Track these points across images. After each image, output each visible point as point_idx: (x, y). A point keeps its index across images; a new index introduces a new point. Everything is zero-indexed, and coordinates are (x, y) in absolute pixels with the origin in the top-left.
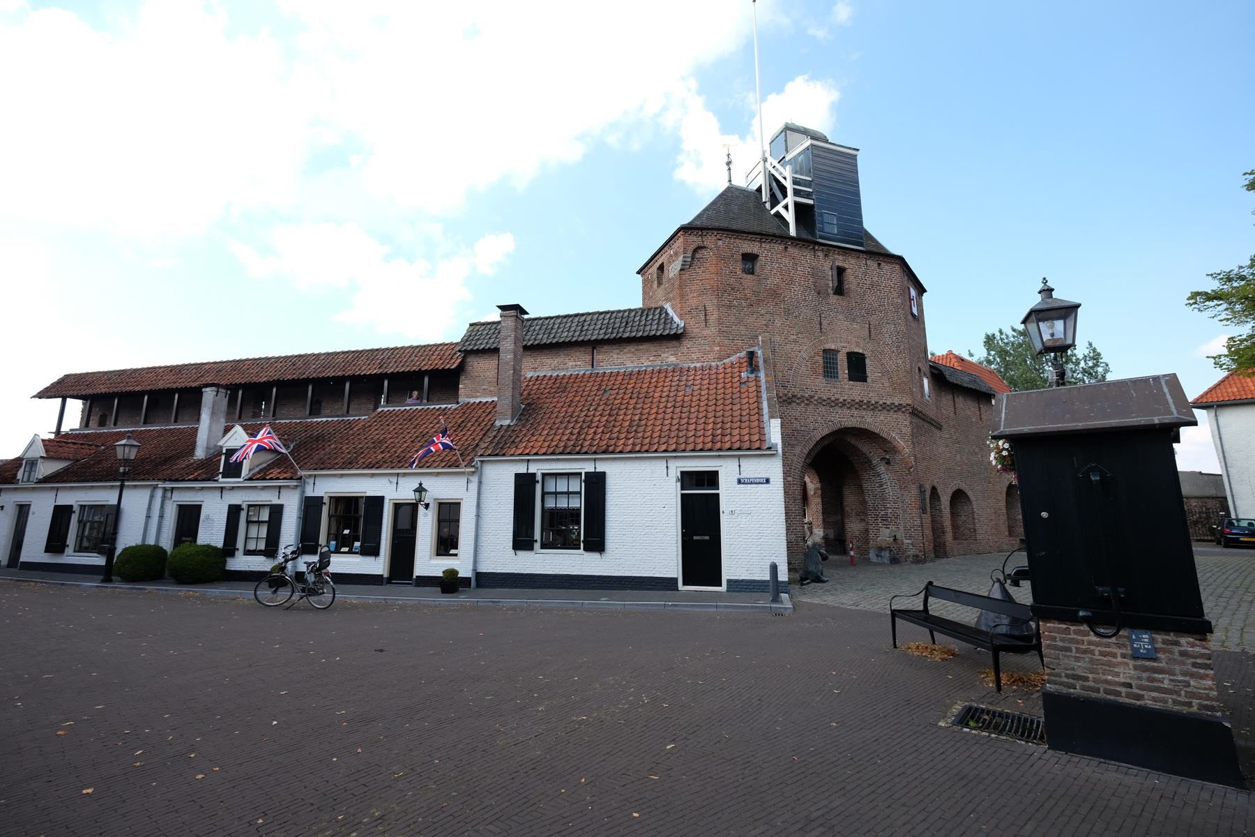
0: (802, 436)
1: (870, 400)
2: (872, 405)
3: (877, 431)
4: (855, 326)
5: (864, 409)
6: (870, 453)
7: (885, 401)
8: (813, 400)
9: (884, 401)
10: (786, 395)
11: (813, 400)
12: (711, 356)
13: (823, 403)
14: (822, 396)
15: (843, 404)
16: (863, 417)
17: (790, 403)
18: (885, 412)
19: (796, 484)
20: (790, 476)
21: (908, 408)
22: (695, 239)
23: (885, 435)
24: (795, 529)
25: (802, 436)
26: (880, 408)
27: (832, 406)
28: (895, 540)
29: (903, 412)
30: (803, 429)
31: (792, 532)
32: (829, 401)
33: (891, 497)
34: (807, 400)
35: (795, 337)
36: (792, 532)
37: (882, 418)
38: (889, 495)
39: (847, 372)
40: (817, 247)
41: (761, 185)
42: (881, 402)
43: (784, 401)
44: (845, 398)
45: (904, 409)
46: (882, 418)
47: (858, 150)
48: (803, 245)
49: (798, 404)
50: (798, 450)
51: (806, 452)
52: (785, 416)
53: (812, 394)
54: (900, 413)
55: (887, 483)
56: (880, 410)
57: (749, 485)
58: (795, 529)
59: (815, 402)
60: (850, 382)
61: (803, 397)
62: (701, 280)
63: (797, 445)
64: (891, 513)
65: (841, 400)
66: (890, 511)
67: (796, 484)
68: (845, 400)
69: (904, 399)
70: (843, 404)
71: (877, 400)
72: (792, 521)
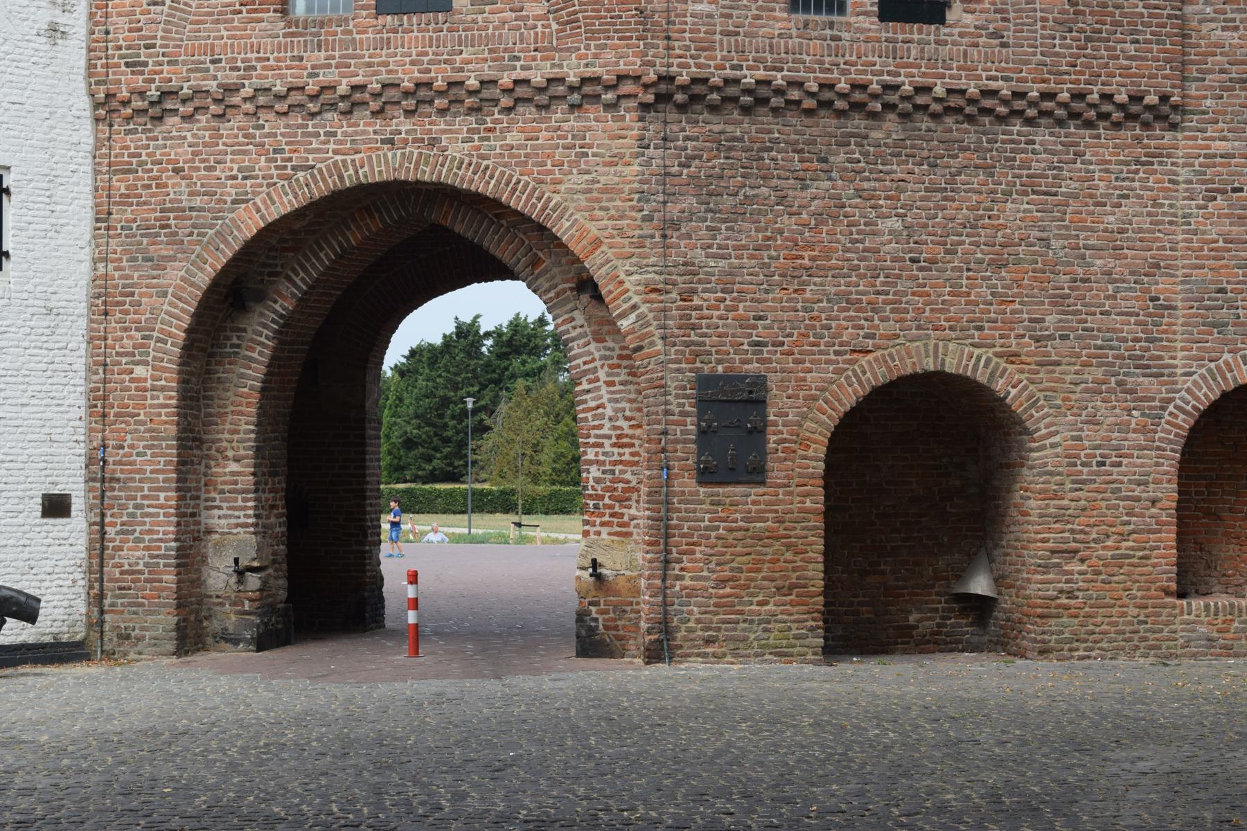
0: (194, 226)
1: (457, 76)
2: (472, 93)
3: (487, 188)
5: (442, 112)
7: (523, 75)
8: (236, 100)
9: (520, 74)
10: (142, 94)
11: (236, 100)
13: (277, 107)
14: (266, 83)
15: (353, 102)
16: (433, 142)
17: (159, 119)
18: (529, 112)
19: (163, 389)
20: (146, 363)
21: (627, 88)
23: (518, 203)
24: (150, 532)
25: (194, 226)
26: (506, 101)
27: (313, 115)
28: (598, 577)
29: (611, 106)
30: (198, 201)
31: (137, 540)
32: (296, 98)
33: (608, 425)
34: (217, 101)
36: (137, 540)
37: (513, 138)
38: (602, 417)
42: (506, 80)
43: (140, 112)
44: (358, 80)
45: (609, 96)
46: (513, 138)
49: (188, 118)
50: (174, 275)
51: (203, 279)
52: (141, 164)
53: (232, 78)
54: (593, 112)
55: (595, 370)
56: (508, 110)
58: (150, 532)
59: (249, 107)
60: (381, 20)
61: (197, 91)
63: (172, 259)
64: (597, 480)
65: (343, 89)
66: (595, 472)
67: (163, 389)
68: (354, 88)
69: (609, 56)
70: (353, 102)
71: (488, 73)
72: (137, 507)
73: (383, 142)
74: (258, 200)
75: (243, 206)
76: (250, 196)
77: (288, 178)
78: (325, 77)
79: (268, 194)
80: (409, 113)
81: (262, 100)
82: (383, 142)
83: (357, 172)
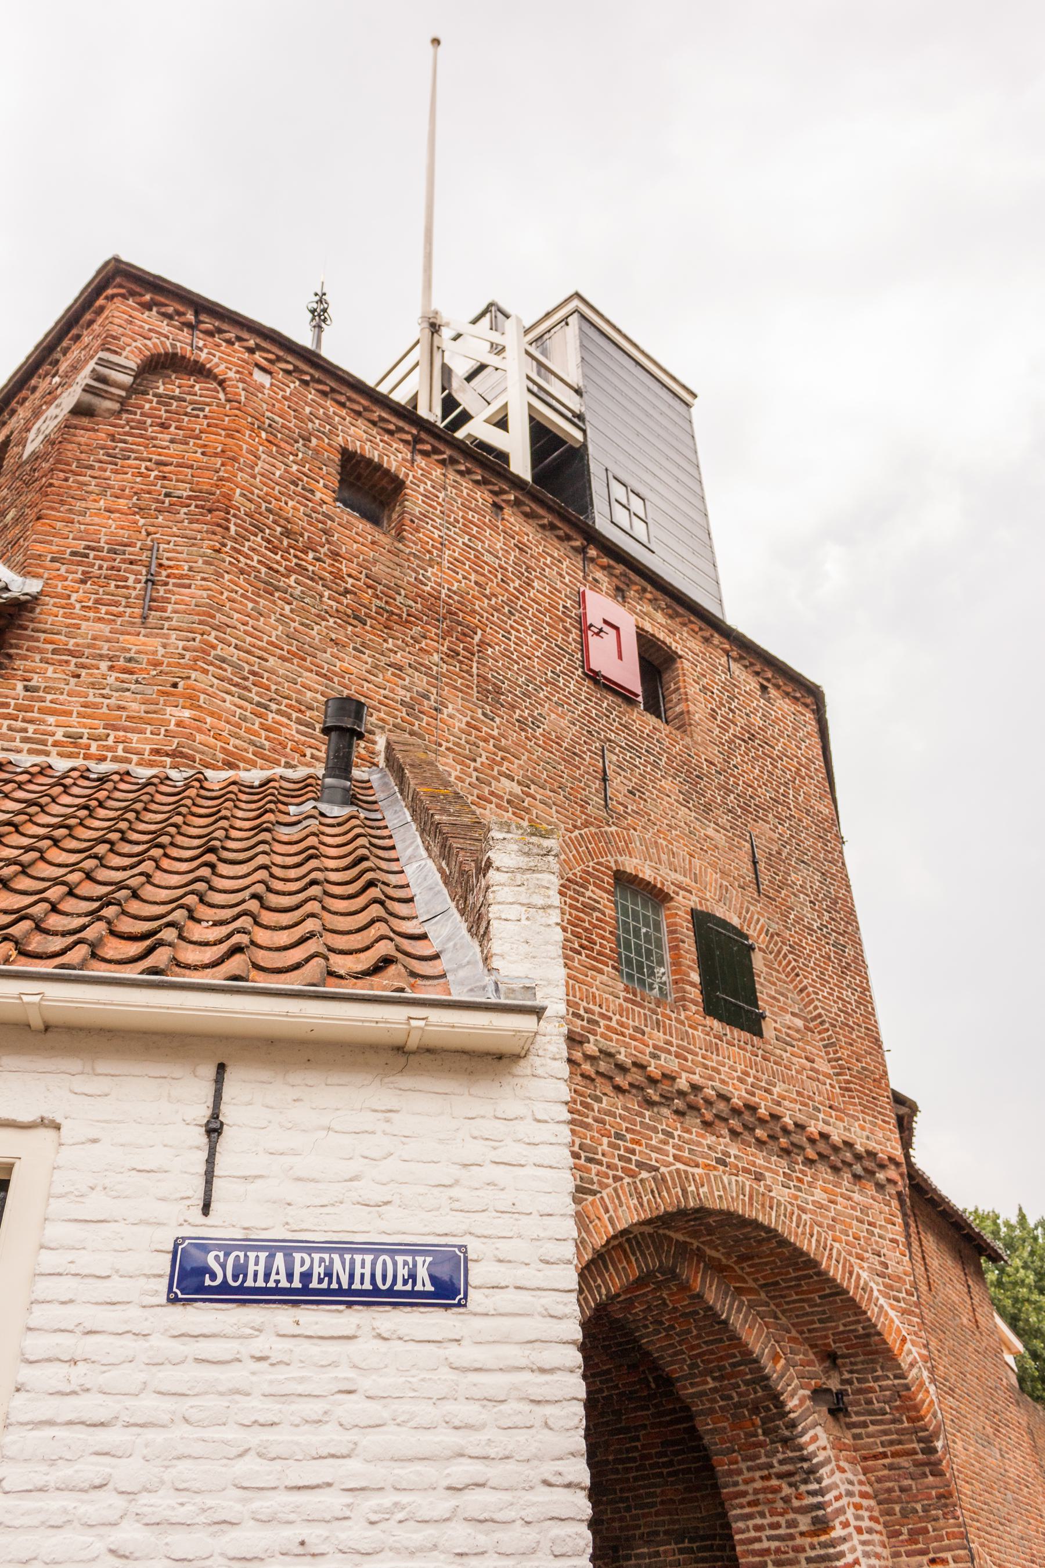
4: (710, 832)
6: (775, 1358)
7: (826, 1129)
12: (142, 742)
13: (619, 1080)
22: (164, 327)
26: (811, 1153)
27: (650, 1103)
35: (517, 790)
39: (695, 977)
40: (592, 552)
41: (416, 395)
42: (813, 1129)
44: (696, 1078)
46: (819, 1195)
47: (695, 396)
48: (552, 527)
56: (809, 1162)
57: (283, 1317)
62: (159, 463)
71: (801, 1118)
73: (718, 1161)
74: (604, 1194)
75: (590, 1198)
76: (595, 1187)
77: (633, 1175)
78: (670, 1063)
79: (615, 1190)
80: (734, 1134)
81: (603, 1066)
82: (718, 1161)
83: (697, 1189)
